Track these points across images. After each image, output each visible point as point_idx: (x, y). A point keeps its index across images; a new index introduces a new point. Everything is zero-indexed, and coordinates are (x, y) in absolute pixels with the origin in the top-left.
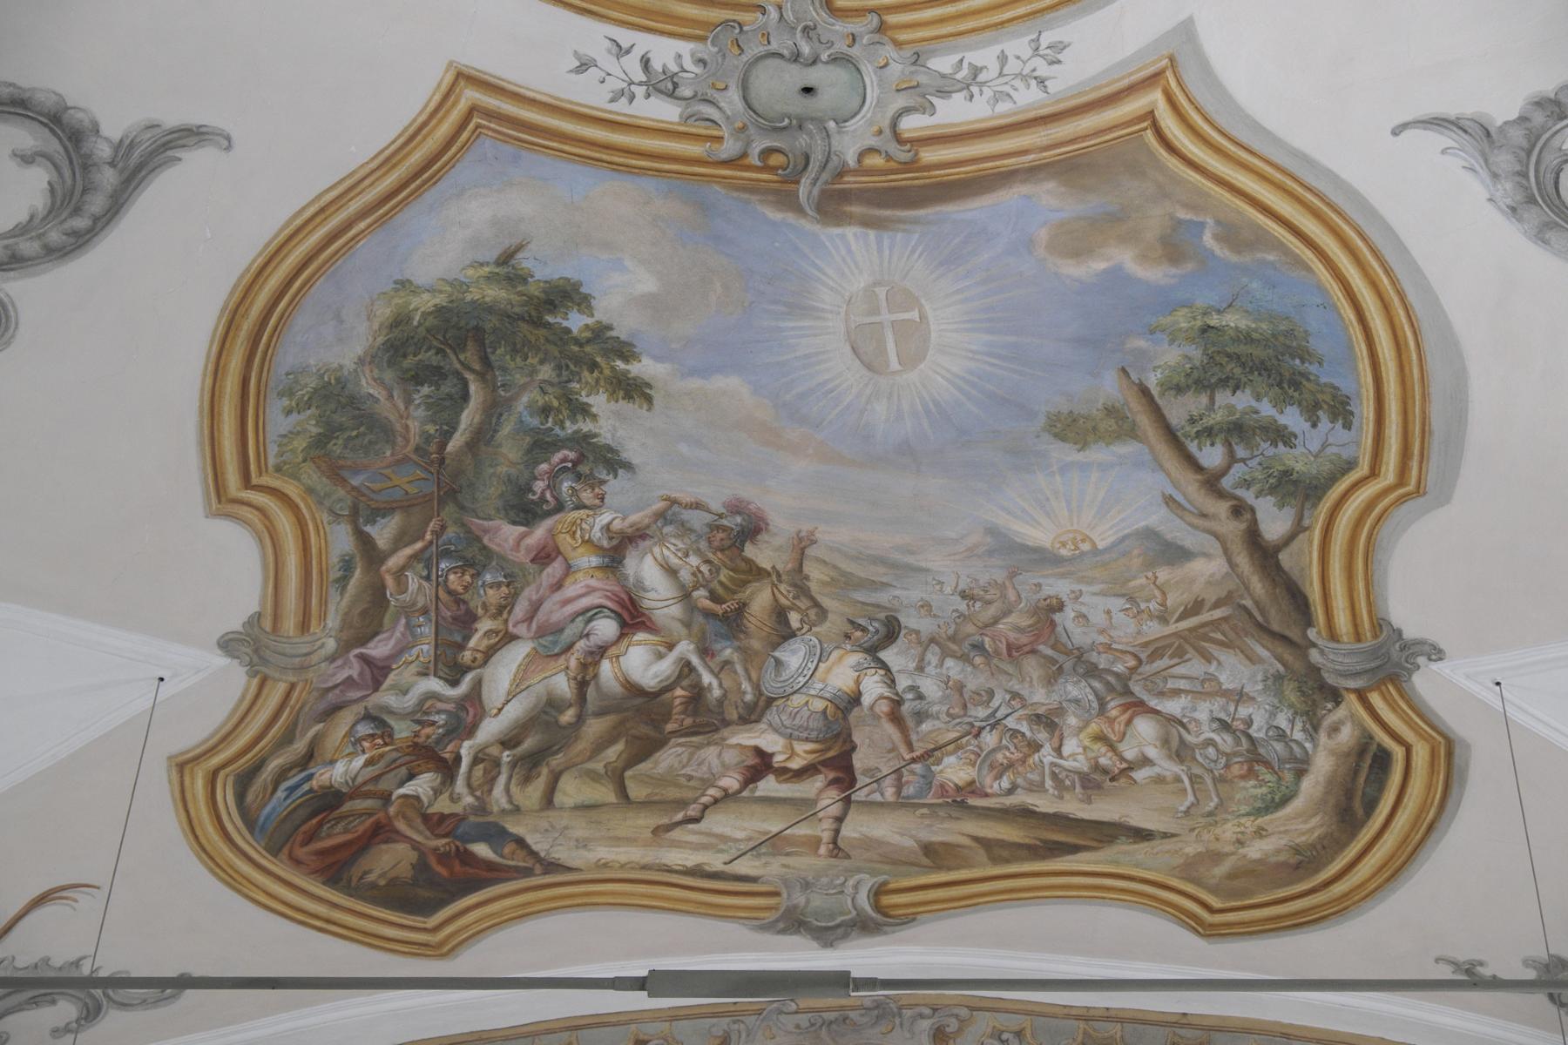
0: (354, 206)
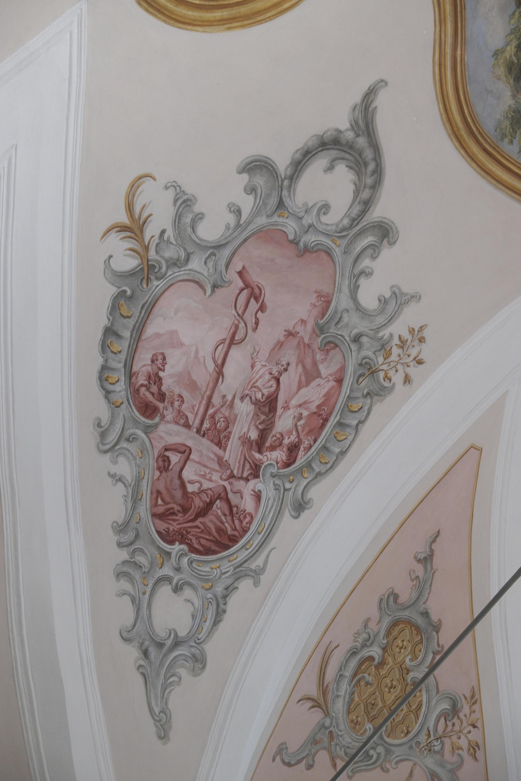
0: (449, 50)
